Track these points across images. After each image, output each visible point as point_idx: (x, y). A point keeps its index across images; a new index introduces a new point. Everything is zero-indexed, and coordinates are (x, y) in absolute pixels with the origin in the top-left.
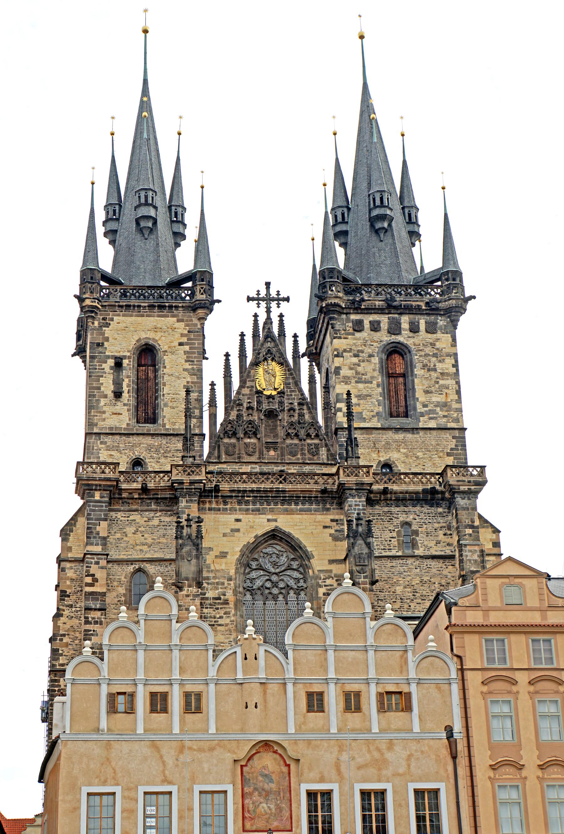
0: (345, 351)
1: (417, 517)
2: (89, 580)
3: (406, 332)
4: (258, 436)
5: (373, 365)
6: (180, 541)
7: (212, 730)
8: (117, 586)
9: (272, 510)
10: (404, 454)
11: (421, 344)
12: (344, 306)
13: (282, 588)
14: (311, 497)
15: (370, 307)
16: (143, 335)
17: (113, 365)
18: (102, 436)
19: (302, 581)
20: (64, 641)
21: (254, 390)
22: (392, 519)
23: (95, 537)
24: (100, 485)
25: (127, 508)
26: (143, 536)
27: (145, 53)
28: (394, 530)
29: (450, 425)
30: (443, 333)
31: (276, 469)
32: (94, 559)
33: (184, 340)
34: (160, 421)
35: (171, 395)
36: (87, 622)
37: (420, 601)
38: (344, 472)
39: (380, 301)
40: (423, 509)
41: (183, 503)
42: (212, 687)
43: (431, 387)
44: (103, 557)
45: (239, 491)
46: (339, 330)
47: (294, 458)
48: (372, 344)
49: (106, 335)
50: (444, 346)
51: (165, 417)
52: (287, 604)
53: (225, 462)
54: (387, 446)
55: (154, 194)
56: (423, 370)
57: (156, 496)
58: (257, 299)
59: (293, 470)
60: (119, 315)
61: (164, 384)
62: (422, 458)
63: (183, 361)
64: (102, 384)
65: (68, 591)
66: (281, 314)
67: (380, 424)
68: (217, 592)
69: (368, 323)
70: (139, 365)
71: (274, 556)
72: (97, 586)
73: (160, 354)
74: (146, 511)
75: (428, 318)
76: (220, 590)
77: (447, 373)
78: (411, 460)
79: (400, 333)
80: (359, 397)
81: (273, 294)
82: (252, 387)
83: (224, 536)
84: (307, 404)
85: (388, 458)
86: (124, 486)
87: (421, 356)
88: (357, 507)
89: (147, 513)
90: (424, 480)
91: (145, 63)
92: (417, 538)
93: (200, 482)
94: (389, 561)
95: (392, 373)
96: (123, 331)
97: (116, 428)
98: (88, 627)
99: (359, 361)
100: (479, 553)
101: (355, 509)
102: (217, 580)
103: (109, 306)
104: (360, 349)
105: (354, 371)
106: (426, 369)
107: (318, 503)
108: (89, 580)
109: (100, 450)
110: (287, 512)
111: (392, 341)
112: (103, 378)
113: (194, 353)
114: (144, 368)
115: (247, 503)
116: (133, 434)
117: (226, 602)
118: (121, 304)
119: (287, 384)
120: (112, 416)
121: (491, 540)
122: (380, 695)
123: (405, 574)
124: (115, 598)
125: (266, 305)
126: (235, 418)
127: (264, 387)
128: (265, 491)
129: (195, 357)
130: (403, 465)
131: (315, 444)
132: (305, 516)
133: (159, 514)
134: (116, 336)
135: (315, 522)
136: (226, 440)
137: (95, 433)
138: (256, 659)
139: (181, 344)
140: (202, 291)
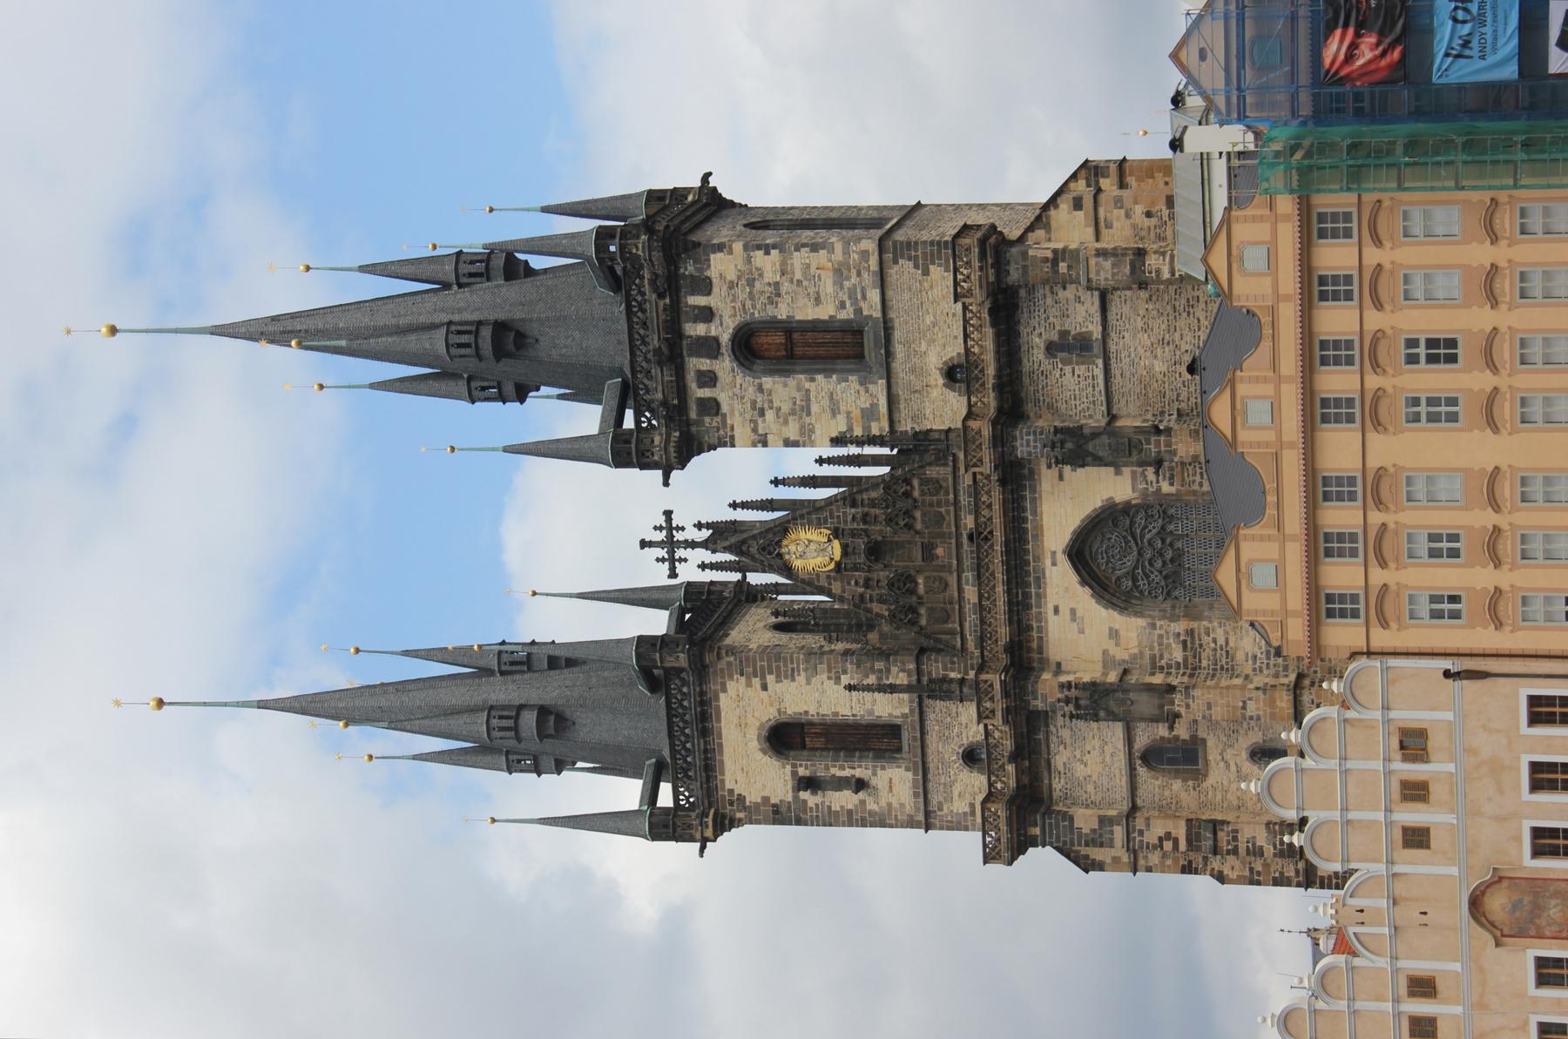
0: (755, 430)
2: (1168, 845)
4: (913, 572)
6: (1102, 714)
7: (1457, 966)
9: (1037, 559)
13: (1163, 541)
16: (754, 744)
23: (1101, 836)
25: (1046, 774)
33: (756, 682)
34: (899, 721)
36: (1235, 852)
37: (1177, 335)
38: (975, 465)
41: (1039, 704)
42: (1401, 964)
45: (1010, 611)
53: (961, 626)
58: (672, 561)
60: (723, 781)
61: (836, 714)
65: (1182, 862)
70: (804, 747)
73: (784, 718)
79: (716, 339)
80: (835, 412)
84: (852, 495)
86: (1012, 783)
87: (754, 307)
91: (226, 704)
93: (1003, 683)
98: (1242, 851)
103: (709, 796)
105: (790, 418)
107: (1023, 487)
108: (1168, 845)
110: (1038, 535)
113: (778, 668)
115: (1027, 595)
116: (924, 763)
117: (1190, 633)
122: (1406, 759)
133: (1052, 728)
136: (923, 622)
137: (926, 818)
139: (765, 687)
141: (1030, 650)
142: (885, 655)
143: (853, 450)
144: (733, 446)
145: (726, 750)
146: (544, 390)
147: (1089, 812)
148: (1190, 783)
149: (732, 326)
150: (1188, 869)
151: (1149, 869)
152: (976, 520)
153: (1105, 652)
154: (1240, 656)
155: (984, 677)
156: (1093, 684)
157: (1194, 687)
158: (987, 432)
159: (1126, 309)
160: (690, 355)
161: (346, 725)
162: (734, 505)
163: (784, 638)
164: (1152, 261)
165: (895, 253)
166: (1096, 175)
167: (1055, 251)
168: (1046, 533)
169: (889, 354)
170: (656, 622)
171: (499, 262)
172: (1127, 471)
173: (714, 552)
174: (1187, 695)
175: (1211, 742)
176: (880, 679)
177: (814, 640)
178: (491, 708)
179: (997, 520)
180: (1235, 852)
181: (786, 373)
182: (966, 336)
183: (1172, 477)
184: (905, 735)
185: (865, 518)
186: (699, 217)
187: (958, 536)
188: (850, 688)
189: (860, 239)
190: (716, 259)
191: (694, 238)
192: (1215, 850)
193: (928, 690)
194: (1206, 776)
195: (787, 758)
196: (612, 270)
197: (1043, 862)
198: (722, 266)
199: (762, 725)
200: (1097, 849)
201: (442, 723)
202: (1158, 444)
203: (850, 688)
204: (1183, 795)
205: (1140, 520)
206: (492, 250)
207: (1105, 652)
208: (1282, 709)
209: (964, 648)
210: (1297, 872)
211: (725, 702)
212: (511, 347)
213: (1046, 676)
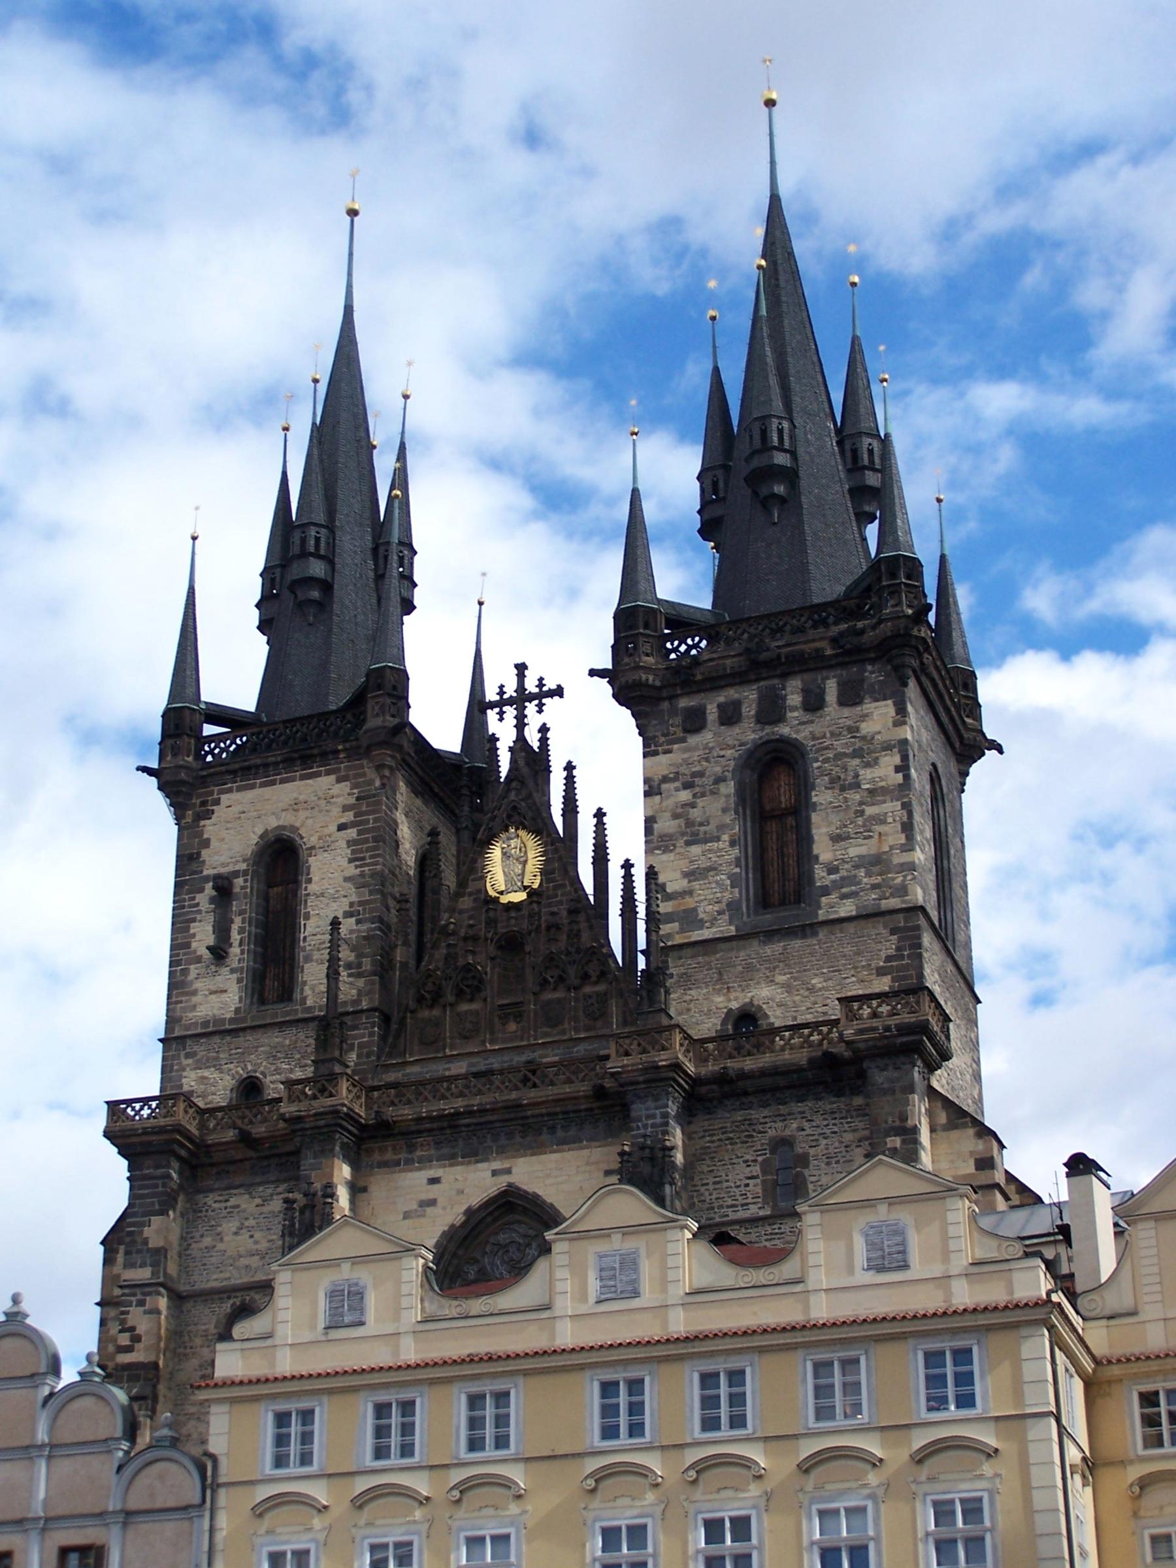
0: (665, 779)
1: (806, 1125)
2: (124, 1339)
3: (796, 714)
5: (723, 799)
8: (202, 1347)
9: (502, 1151)
10: (783, 986)
11: (828, 735)
12: (658, 683)
14: (580, 1111)
15: (714, 674)
16: (273, 823)
18: (189, 1042)
21: (482, 896)
22: (752, 1136)
23: (139, 1252)
24: (150, 1143)
26: (252, 1236)
28: (755, 1161)
29: (886, 904)
30: (877, 700)
31: (519, 1059)
32: (134, 1295)
33: (349, 817)
34: (297, 996)
35: (319, 937)
39: (734, 656)
43: (846, 826)
48: (722, 753)
49: (205, 836)
50: (877, 728)
51: (305, 983)
54: (748, 975)
56: (830, 791)
57: (275, 1151)
59: (551, 1057)
60: (230, 791)
61: (307, 917)
62: (820, 989)
63: (344, 862)
64: (194, 935)
67: (733, 928)
73: (303, 854)
74: (260, 1184)
75: (844, 673)
78: (797, 998)
79: (780, 719)
80: (690, 875)
81: (531, 686)
82: (479, 891)
83: (404, 1218)
85: (747, 1000)
88: (650, 1122)
89: (261, 1189)
90: (815, 1038)
92: (806, 1172)
94: (743, 1230)
95: (773, 810)
96: (238, 822)
97: (219, 1021)
99: (694, 796)
105: (682, 822)
108: (124, 1339)
109: (184, 1070)
111: (764, 739)
112: (196, 924)
113: (366, 841)
114: (280, 888)
116: (244, 1029)
119: (545, 873)
124: (195, 1370)
125: (515, 712)
127: (503, 888)
128: (482, 1111)
130: (778, 1012)
131: (598, 994)
132: (568, 1155)
134: (224, 834)
135: (588, 1164)
139: (342, 827)
140: (377, 708)
141: (382, 1150)
144: (645, 755)
145: (267, 791)
147: (174, 1238)
149: (800, 737)
151: (103, 1322)
167: (915, 1130)
169: (769, 935)
170: (438, 720)
171: (872, 479)
176: (349, 966)
179: (550, 1092)
182: (795, 1028)
184: (281, 1008)
185: (553, 927)
186: (945, 719)
190: (886, 709)
198: (878, 717)
199: (298, 829)
201: (317, 479)
203: (335, 924)
211: (325, 782)
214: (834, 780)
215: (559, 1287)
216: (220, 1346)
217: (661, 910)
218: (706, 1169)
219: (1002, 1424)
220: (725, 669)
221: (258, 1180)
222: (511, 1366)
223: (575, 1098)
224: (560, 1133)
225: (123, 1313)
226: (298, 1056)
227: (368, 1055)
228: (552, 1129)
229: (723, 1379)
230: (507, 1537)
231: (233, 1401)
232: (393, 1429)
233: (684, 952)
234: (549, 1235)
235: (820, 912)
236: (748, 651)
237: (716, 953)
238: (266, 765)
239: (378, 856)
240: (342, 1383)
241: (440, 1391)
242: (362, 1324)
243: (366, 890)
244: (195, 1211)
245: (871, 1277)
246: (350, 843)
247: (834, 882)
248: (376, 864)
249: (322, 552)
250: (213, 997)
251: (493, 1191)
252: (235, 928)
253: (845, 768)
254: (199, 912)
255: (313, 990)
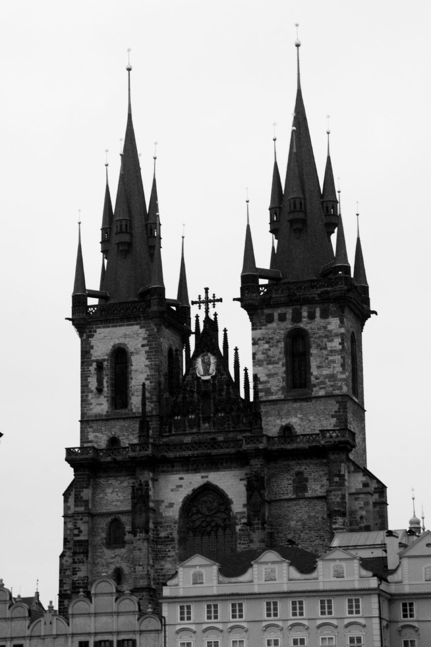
0: (259, 339)
2: (76, 532)
3: (305, 320)
5: (280, 349)
6: (135, 501)
9: (205, 470)
12: (257, 304)
13: (213, 527)
16: (117, 342)
17: (96, 367)
19: (227, 520)
20: (67, 574)
23: (80, 501)
26: (117, 495)
27: (129, 90)
28: (290, 479)
30: (333, 317)
32: (79, 516)
33: (145, 342)
34: (129, 408)
37: (307, 531)
38: (246, 441)
40: (312, 461)
44: (85, 515)
46: (255, 323)
47: (222, 428)
48: (280, 331)
49: (92, 344)
52: (217, 538)
53: (174, 435)
54: (288, 414)
55: (128, 222)
58: (199, 302)
60: (100, 327)
63: (144, 359)
64: (89, 382)
65: (69, 538)
66: (216, 313)
67: (283, 396)
68: (167, 532)
69: (277, 315)
71: (208, 502)
72: (82, 536)
74: (120, 476)
76: (169, 531)
77: (335, 350)
79: (300, 321)
81: (211, 297)
85: (288, 423)
86: (102, 460)
87: (315, 338)
88: (256, 466)
91: (129, 99)
92: (307, 484)
96: (104, 340)
97: (100, 415)
98: (75, 565)
99: (270, 346)
100: (340, 496)
101: (255, 468)
102: (167, 524)
104: (271, 336)
106: (319, 348)
108: (76, 532)
111: (295, 328)
112: (90, 378)
113: (152, 352)
116: (110, 419)
117: (173, 540)
118: (100, 319)
119: (217, 369)
120: (97, 407)
121: (362, 481)
123: (297, 511)
124: (99, 541)
126: (181, 400)
128: (198, 456)
129: (153, 355)
130: (298, 427)
132: (227, 472)
134: (98, 344)
135: (234, 476)
137: (85, 421)
138: (51, 624)
139: (143, 346)
142: (159, 401)
143: (251, 385)
144: (253, 329)
145: (114, 329)
146: (276, 241)
147: (90, 495)
148: (105, 541)
149: (307, 328)
150: (66, 541)
151: (65, 523)
152: (222, 442)
153: (163, 501)
154: (163, 563)
155: (150, 446)
156: (148, 496)
157: (148, 542)
158: (261, 446)
159: (318, 508)
160: (292, 309)
161: (121, 155)
162: (225, 330)
163: (166, 354)
164: (340, 520)
165: (342, 402)
166: (380, 492)
167: (344, 475)
168: (216, 473)
169: (295, 400)
170: (171, 293)
172: (245, 510)
173: (204, 321)
174: (144, 539)
175: (123, 550)
176: (148, 398)
177: (165, 368)
178: (131, 221)
179: (222, 451)
180: (74, 562)
181: (287, 352)
183: (243, 530)
187: (215, 433)
188: (144, 385)
189: (347, 385)
191: (346, 310)
192: (75, 553)
193: (144, 420)
194: (108, 548)
195: (111, 357)
196: (330, 273)
197: (68, 475)
198: (334, 324)
199: (125, 345)
200: (73, 499)
202: (258, 524)
203: (144, 385)
204: (99, 538)
205: (224, 516)
206: (339, 218)
207: (163, 501)
208: (139, 582)
209: (163, 437)
210: (66, 590)
211: (136, 328)
212: (295, 227)
213: (151, 475)
214: (318, 346)
215: (255, 576)
216: (164, 587)
217: (259, 388)
218: (274, 480)
219: (366, 619)
220: (281, 301)
221: (118, 475)
222: (243, 597)
223: (229, 454)
224: (225, 465)
225: (75, 523)
226: (130, 430)
227: (156, 432)
228: (222, 464)
229: (297, 603)
230: (243, 641)
231: (168, 603)
232: (212, 612)
233: (266, 403)
234: (252, 563)
235: (313, 393)
236: (289, 296)
237: (277, 405)
238: (113, 319)
239: (157, 358)
240: (199, 599)
241: (224, 602)
242: (202, 583)
243: (153, 371)
244: (96, 484)
245: (335, 579)
246: (146, 352)
247: (318, 383)
248: (156, 361)
249: (128, 231)
250: (98, 406)
251: (202, 483)
252: (105, 381)
253: (322, 341)
254: (91, 374)
255: (135, 406)
